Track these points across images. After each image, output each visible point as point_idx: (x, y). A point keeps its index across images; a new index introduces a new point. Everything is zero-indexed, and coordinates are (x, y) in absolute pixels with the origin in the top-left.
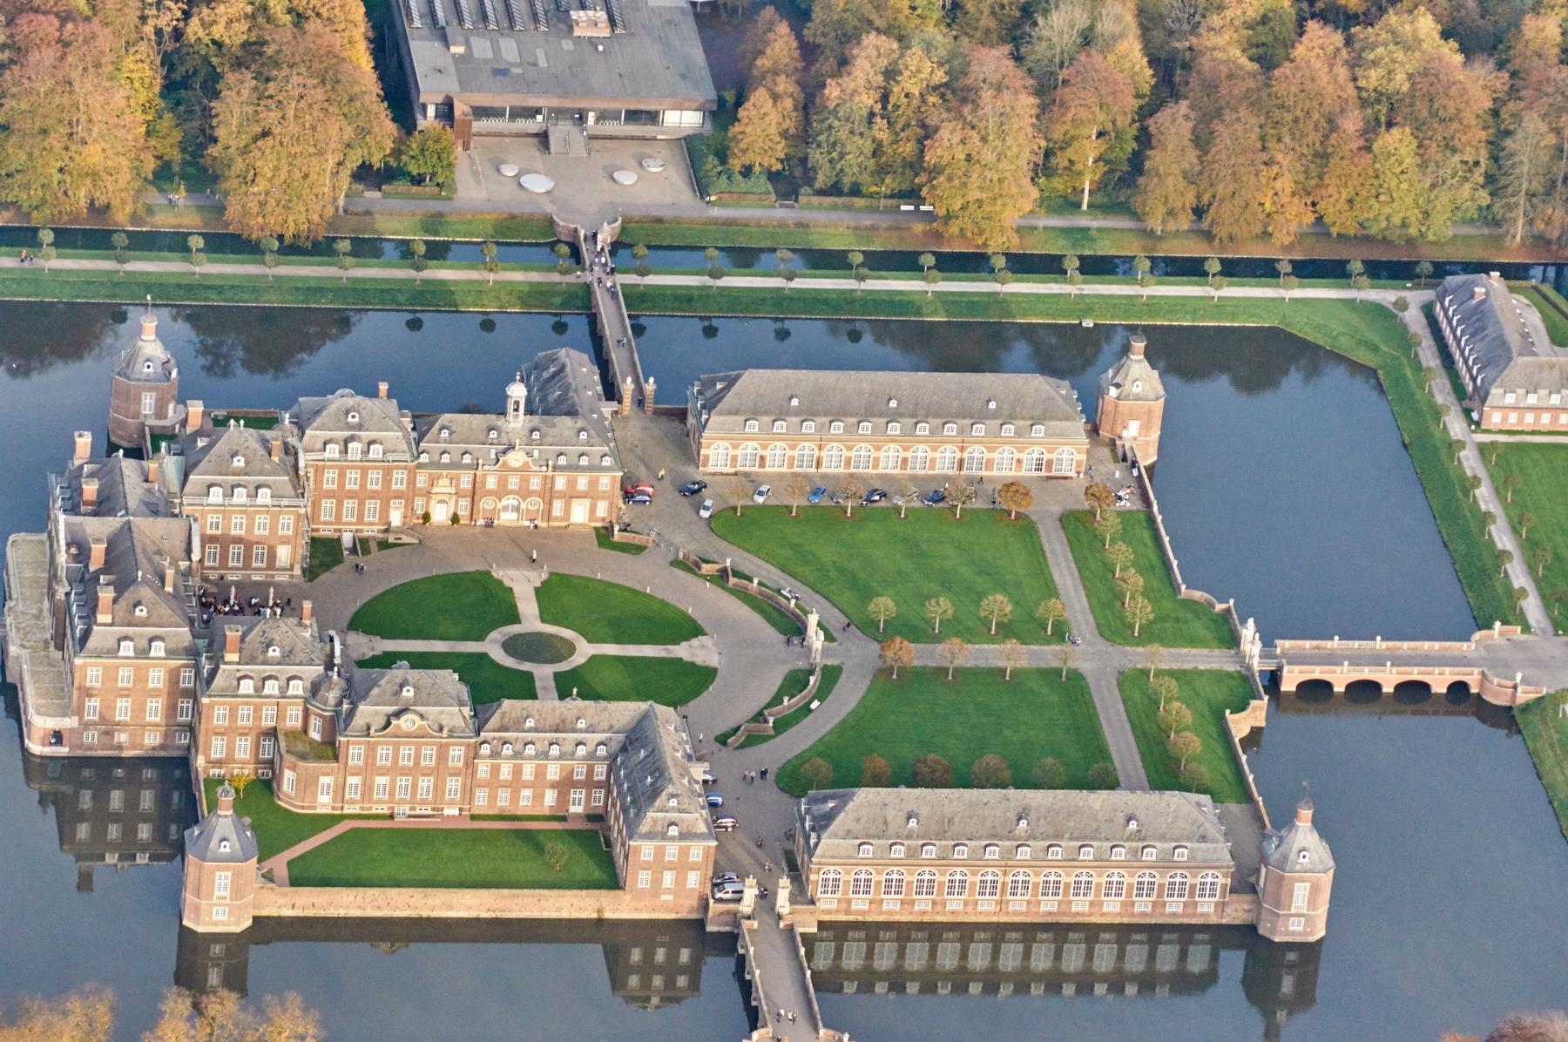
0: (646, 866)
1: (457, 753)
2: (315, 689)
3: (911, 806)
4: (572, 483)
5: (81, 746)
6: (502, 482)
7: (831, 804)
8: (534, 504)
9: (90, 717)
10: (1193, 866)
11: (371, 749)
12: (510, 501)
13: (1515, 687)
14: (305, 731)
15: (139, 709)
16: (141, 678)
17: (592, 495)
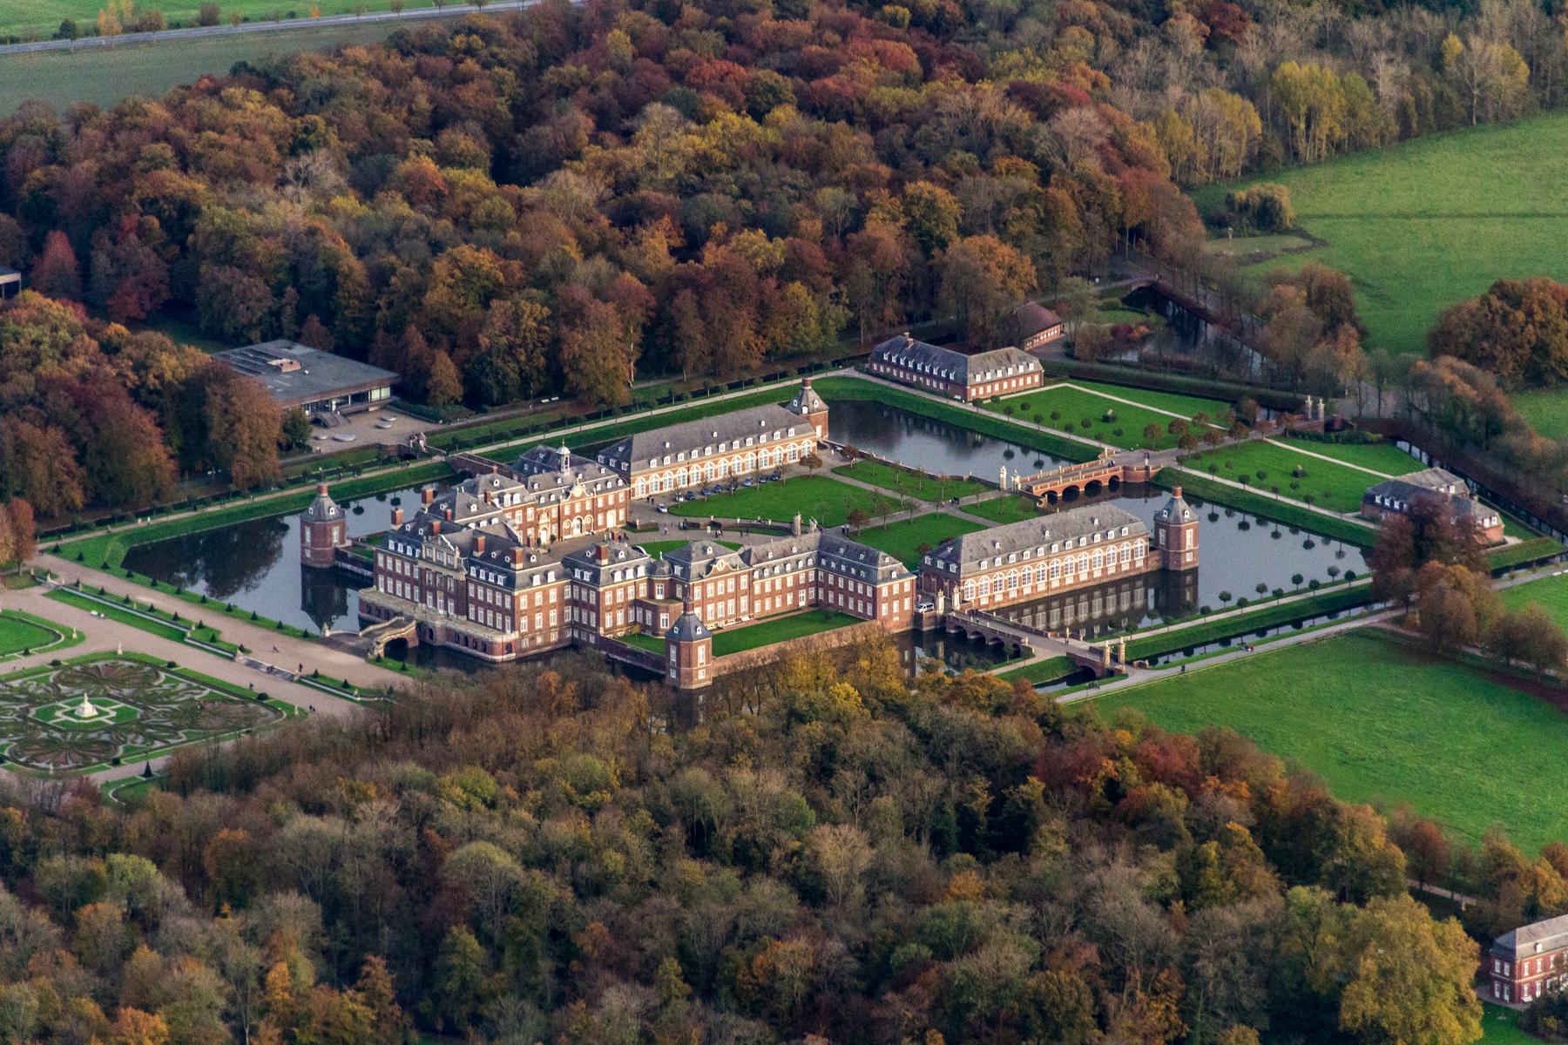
0: (886, 600)
1: (744, 580)
2: (651, 570)
3: (991, 538)
4: (606, 501)
5: (522, 651)
6: (572, 506)
7: (950, 549)
8: (587, 520)
9: (524, 630)
10: (1132, 538)
11: (704, 586)
12: (576, 522)
13: (1147, 468)
14: (651, 595)
15: (546, 619)
16: (546, 597)
17: (616, 506)
